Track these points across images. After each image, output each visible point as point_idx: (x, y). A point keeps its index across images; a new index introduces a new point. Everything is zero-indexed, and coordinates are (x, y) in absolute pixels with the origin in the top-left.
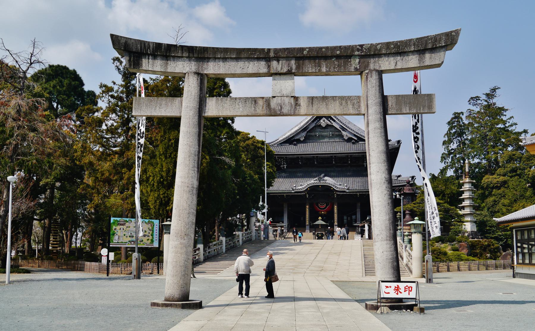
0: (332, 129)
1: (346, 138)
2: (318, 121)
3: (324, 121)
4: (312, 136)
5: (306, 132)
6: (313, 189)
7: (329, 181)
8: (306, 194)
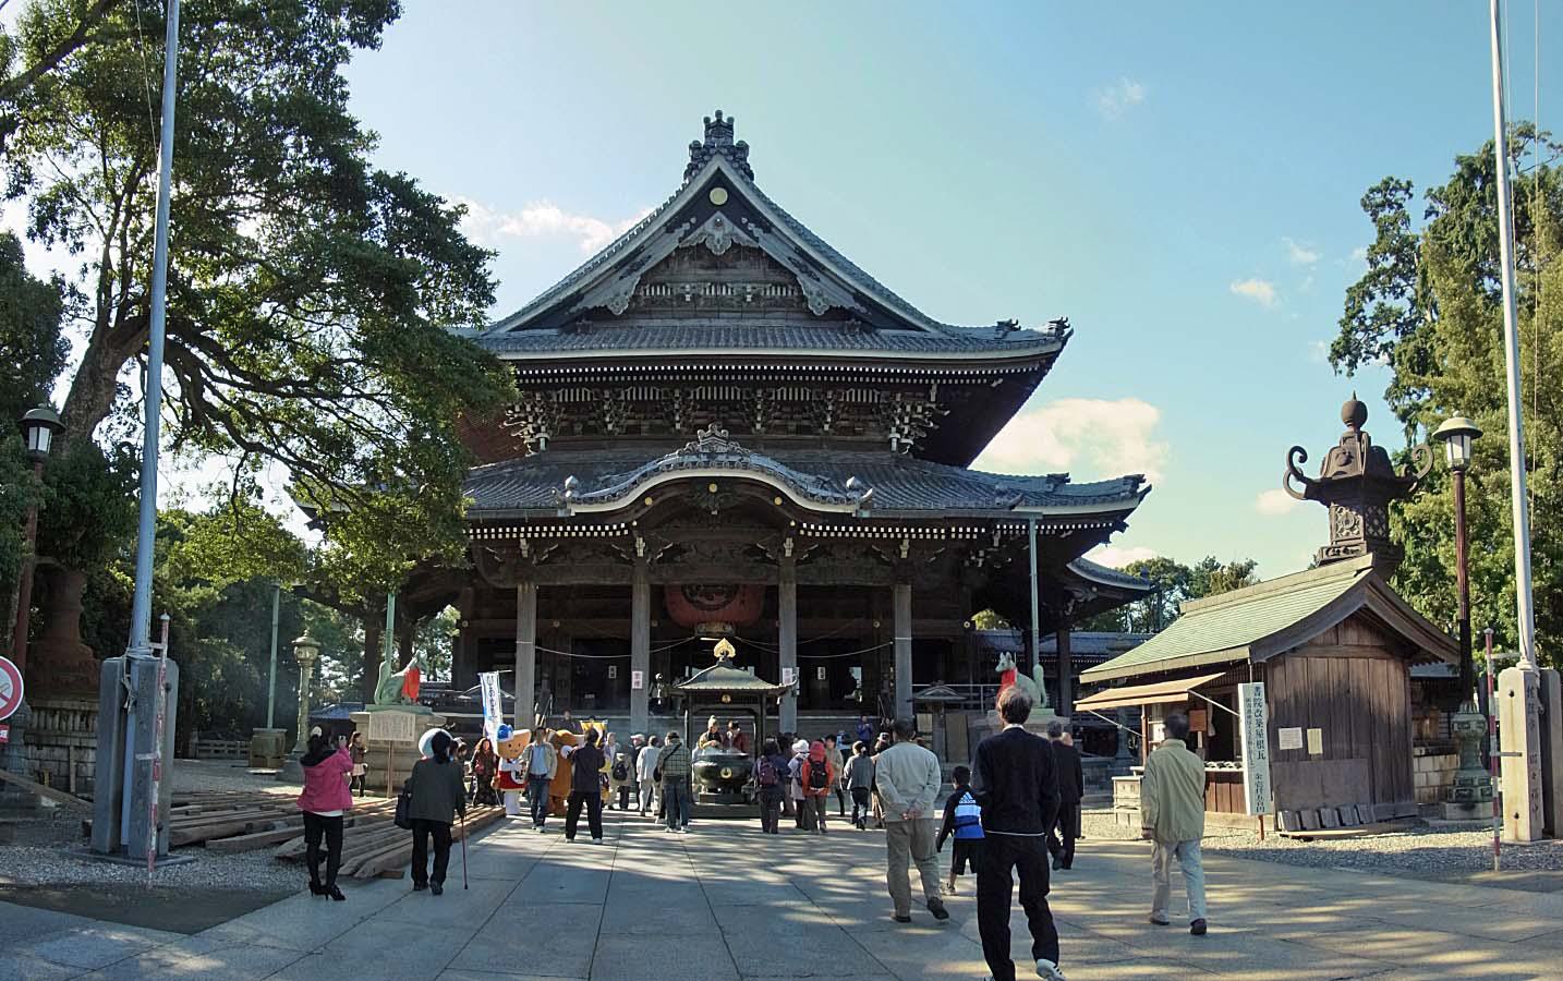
0: (758, 271)
1: (818, 307)
2: (694, 227)
3: (718, 225)
4: (663, 302)
5: (636, 278)
6: (678, 507)
7: (761, 469)
8: (630, 542)
